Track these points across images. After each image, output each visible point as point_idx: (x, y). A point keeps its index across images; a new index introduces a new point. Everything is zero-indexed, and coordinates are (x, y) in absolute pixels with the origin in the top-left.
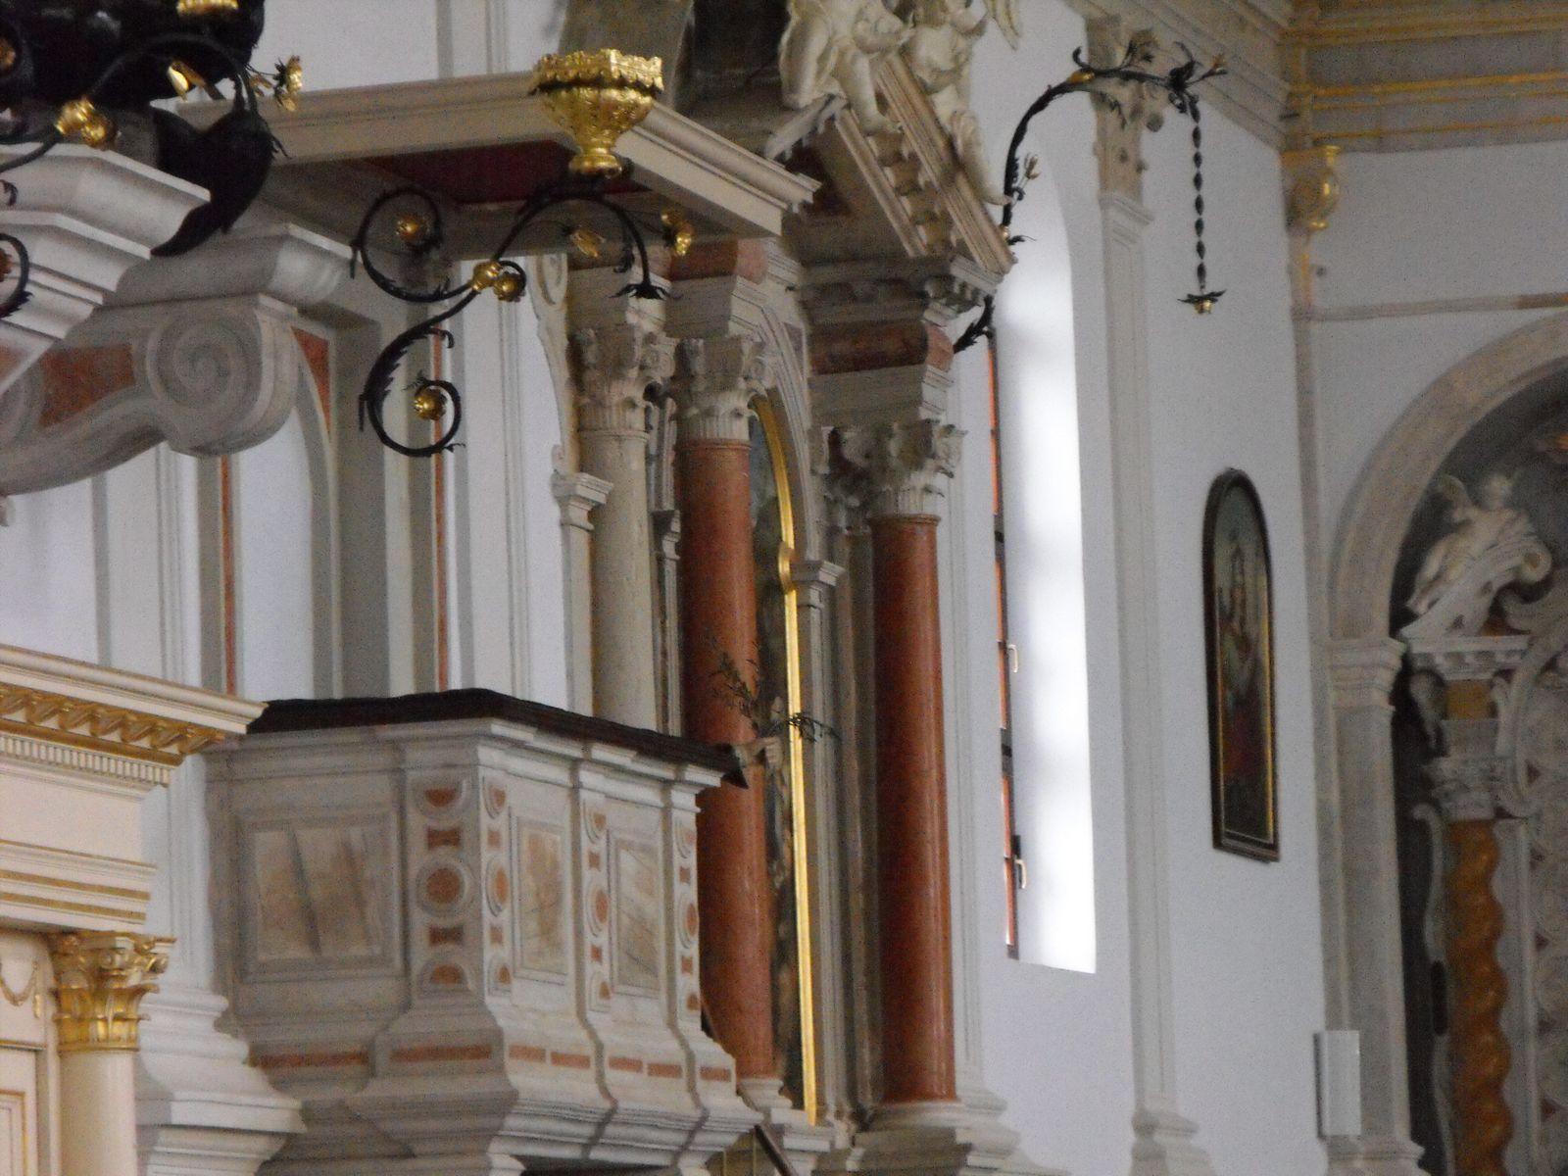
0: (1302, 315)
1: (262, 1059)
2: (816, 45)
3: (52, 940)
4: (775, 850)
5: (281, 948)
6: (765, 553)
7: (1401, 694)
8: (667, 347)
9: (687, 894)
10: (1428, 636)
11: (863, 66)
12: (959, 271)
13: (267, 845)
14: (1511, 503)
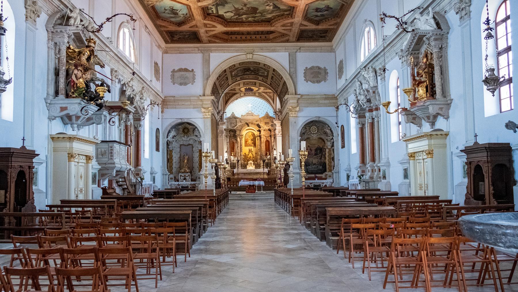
0: (162, 119)
1: (98, 164)
3: (86, 156)
5: (100, 156)
7: (167, 142)
9: (126, 154)
10: (169, 138)
13: (99, 150)
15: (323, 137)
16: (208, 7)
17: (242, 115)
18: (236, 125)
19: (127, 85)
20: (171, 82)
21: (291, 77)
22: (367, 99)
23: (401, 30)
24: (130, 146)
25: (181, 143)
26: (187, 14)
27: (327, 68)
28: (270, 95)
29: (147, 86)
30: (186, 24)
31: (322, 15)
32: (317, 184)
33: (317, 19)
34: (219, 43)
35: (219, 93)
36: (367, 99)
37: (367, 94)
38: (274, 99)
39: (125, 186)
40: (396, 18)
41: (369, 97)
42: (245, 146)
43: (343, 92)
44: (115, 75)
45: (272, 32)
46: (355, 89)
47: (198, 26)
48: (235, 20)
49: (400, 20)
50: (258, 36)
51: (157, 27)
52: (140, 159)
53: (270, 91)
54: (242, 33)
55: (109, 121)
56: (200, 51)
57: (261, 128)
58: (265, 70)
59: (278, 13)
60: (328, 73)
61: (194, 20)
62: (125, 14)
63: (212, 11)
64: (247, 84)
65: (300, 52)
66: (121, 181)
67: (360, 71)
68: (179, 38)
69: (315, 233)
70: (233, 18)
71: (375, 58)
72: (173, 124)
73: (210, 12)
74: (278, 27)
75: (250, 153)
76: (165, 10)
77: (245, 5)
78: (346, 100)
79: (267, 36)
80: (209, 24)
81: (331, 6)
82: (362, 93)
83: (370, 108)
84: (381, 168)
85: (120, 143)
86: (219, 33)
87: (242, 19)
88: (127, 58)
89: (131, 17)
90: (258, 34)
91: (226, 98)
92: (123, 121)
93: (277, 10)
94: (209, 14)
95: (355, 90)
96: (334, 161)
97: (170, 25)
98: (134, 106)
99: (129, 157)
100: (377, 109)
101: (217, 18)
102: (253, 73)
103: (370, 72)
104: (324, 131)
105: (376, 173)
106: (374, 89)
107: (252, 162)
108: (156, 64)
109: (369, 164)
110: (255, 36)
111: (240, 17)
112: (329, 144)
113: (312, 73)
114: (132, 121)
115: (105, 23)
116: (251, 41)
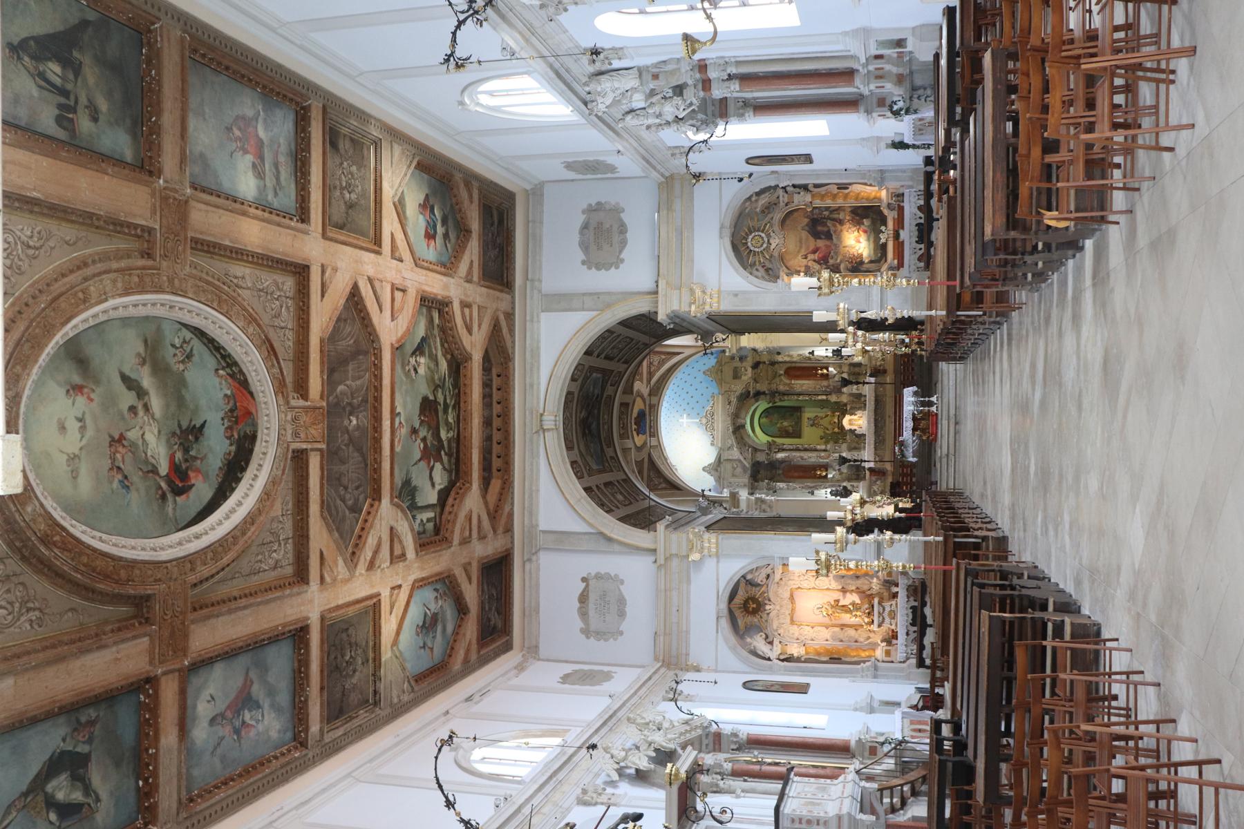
0: (716, 671)
2: (664, 744)
4: (806, 767)
6: (753, 763)
7: (783, 660)
8: (715, 776)
9: (812, 780)
10: (773, 655)
11: (669, 736)
12: (705, 725)
14: (751, 637)
15: (778, 216)
16: (419, 533)
17: (712, 444)
18: (740, 461)
19: (622, 764)
20: (615, 639)
21: (608, 306)
22: (675, 94)
23: (489, 9)
24: (793, 768)
25: (788, 618)
26: (436, 590)
27: (585, 206)
28: (656, 363)
29: (625, 709)
30: (461, 592)
31: (444, 222)
32: (916, 233)
33: (452, 236)
34: (512, 504)
35: (649, 507)
36: (675, 94)
37: (659, 97)
38: (669, 353)
39: (906, 788)
40: (458, 27)
41: (670, 91)
42: (799, 436)
43: (651, 160)
44: (595, 795)
45: (486, 358)
46: (644, 127)
47: (467, 560)
48: (453, 461)
49: (462, 17)
50: (496, 396)
51: (469, 668)
52: (828, 742)
53: (645, 363)
54: (488, 439)
55: (721, 823)
56: (534, 558)
57: (751, 390)
58: (586, 378)
59: (435, 343)
60: (599, 203)
61: (450, 570)
62: (436, 758)
63: (429, 520)
64: (624, 426)
65: (540, 281)
66: (892, 798)
67: (596, 115)
68: (499, 613)
69: (1058, 264)
70: (447, 466)
71: (562, 79)
72: (733, 639)
73: (430, 526)
74: (474, 344)
75: (822, 422)
76: (424, 647)
77: (414, 431)
78: (675, 151)
79: (494, 372)
80: (463, 530)
81: (422, 198)
82: (657, 109)
83: (700, 86)
84: (874, 51)
85: (782, 796)
86: (486, 503)
87: (449, 441)
88: (548, 760)
89: (443, 743)
90: (490, 396)
91: (661, 489)
92: (721, 783)
93: (430, 346)
94: (437, 530)
95: (648, 127)
96: (850, 184)
97: (464, 635)
98: (680, 751)
99: (821, 772)
100: (702, 67)
101: (447, 509)
102: (596, 411)
103: (599, 89)
104: (763, 212)
105: (888, 67)
106: (648, 77)
107: (848, 417)
108: (566, 679)
109: (861, 87)
110: (495, 403)
111: (445, 443)
112: (801, 199)
113: (599, 248)
114: (721, 756)
115: (458, 814)
116: (506, 415)
